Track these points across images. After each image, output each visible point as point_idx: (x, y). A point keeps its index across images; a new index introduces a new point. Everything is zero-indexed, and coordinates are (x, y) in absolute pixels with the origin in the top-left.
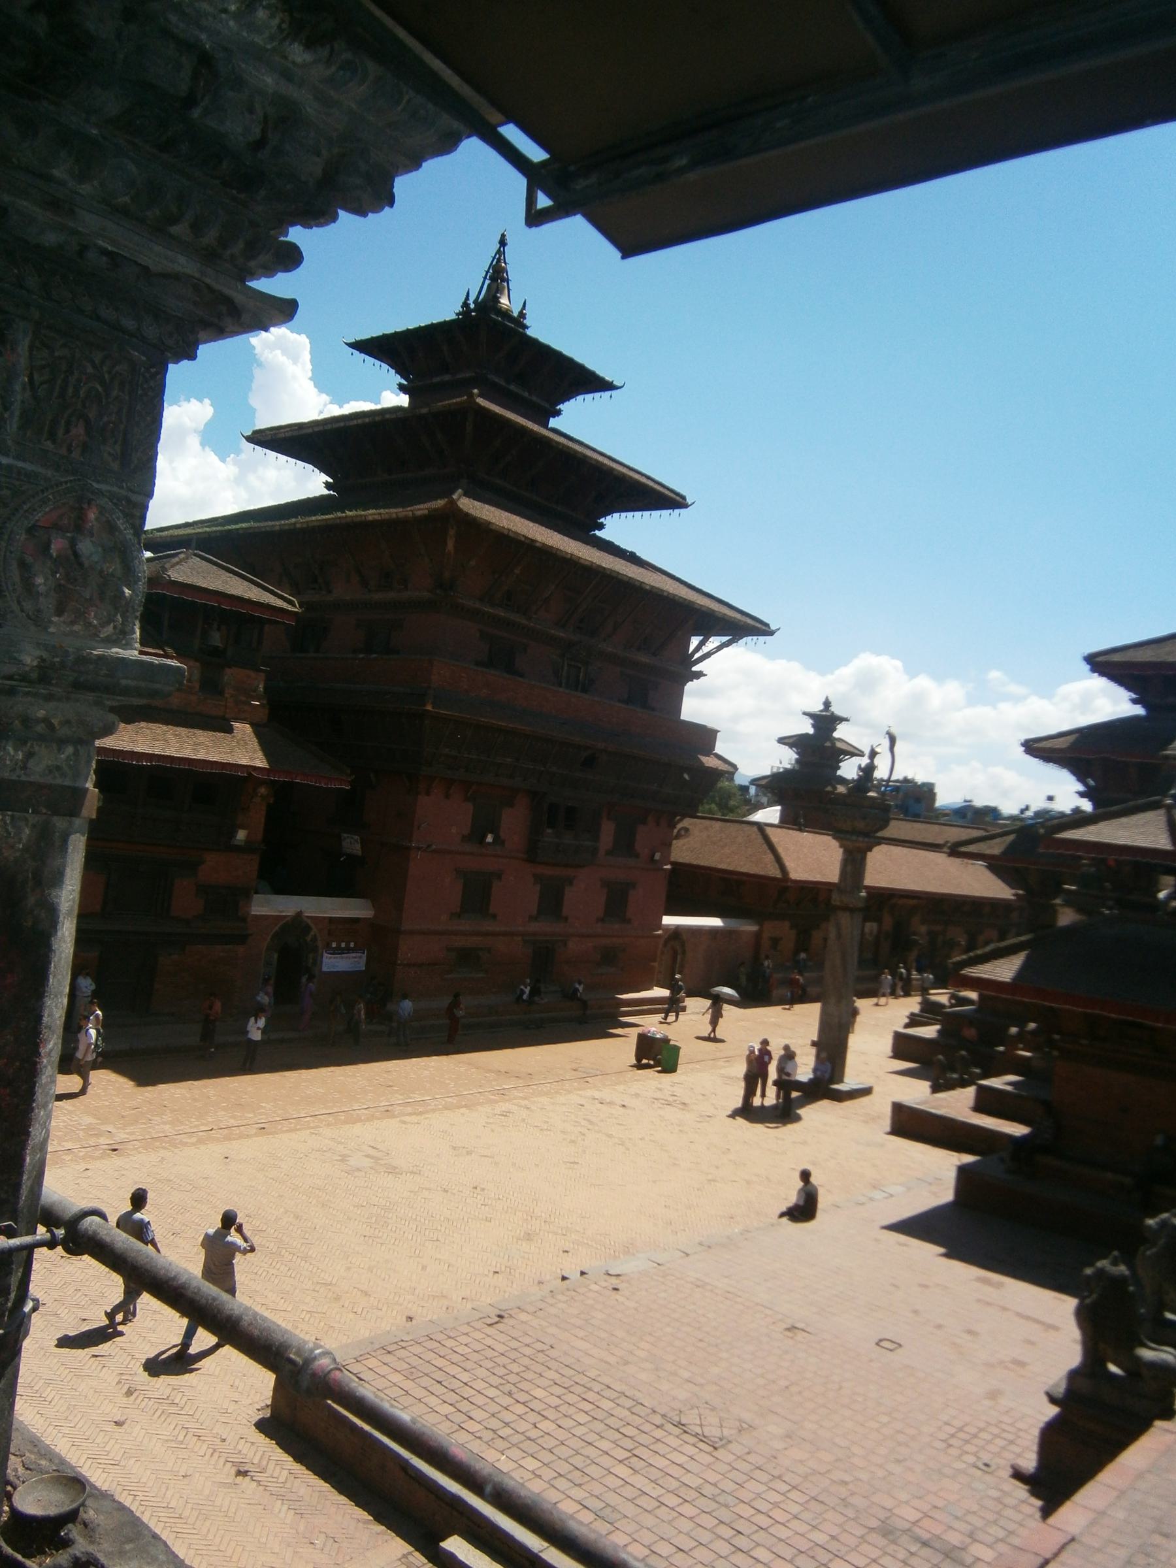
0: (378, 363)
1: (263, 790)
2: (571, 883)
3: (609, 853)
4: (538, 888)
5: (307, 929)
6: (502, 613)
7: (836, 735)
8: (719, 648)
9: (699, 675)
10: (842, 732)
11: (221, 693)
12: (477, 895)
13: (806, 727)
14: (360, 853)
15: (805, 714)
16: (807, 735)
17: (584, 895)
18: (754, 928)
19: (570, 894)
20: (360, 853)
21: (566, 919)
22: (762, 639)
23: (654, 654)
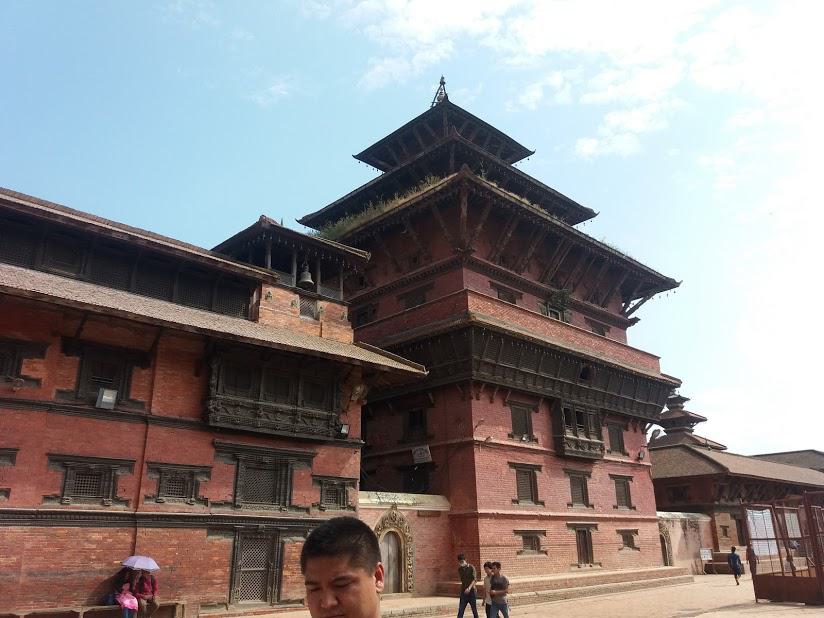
2: (590, 476)
8: (642, 302)
9: (636, 320)
10: (687, 407)
11: (317, 319)
14: (430, 459)
17: (600, 482)
19: (591, 484)
21: (592, 506)
22: (673, 290)
23: (603, 306)
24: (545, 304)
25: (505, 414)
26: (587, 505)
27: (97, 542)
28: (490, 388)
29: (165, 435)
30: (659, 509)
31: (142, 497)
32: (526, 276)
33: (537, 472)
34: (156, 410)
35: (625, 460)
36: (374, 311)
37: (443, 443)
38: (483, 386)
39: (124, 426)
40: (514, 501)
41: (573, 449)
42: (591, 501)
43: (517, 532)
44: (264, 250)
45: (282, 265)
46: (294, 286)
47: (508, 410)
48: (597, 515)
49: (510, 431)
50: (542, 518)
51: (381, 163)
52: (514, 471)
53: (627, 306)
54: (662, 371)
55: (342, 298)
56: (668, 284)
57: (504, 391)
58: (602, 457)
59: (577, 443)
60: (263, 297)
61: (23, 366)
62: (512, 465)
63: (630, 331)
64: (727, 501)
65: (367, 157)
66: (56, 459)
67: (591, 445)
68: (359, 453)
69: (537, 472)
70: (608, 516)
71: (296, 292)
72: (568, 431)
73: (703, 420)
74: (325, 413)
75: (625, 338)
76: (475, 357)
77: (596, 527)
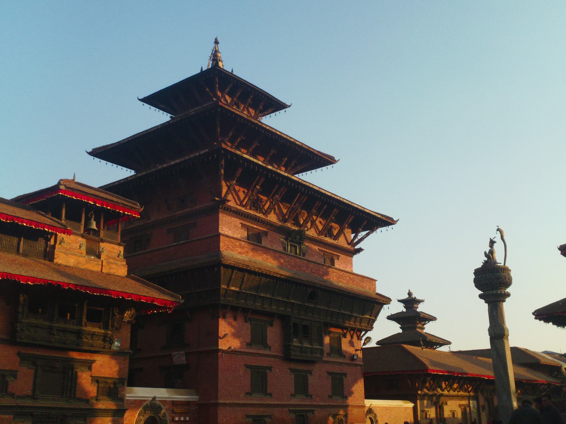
1: (127, 315)
3: (329, 354)
4: (293, 376)
5: (160, 408)
6: (252, 212)
7: (418, 310)
8: (367, 235)
9: (360, 250)
10: (421, 308)
11: (99, 257)
12: (259, 380)
13: (400, 308)
14: (185, 362)
15: (399, 301)
16: (403, 312)
18: (411, 405)
19: (311, 380)
21: (311, 396)
24: (286, 239)
25: (247, 328)
30: (368, 397)
33: (268, 371)
38: (229, 308)
40: (247, 393)
41: (298, 353)
42: (310, 391)
43: (248, 416)
44: (61, 204)
45: (73, 217)
46: (82, 232)
47: (248, 325)
48: (315, 403)
49: (248, 340)
52: (249, 370)
53: (355, 237)
54: (378, 291)
55: (119, 241)
57: (245, 311)
59: (301, 349)
60: (58, 242)
62: (247, 366)
63: (356, 258)
67: (312, 351)
68: (128, 360)
69: (268, 371)
70: (323, 404)
71: (83, 236)
74: (103, 331)
75: (351, 264)
77: (313, 411)
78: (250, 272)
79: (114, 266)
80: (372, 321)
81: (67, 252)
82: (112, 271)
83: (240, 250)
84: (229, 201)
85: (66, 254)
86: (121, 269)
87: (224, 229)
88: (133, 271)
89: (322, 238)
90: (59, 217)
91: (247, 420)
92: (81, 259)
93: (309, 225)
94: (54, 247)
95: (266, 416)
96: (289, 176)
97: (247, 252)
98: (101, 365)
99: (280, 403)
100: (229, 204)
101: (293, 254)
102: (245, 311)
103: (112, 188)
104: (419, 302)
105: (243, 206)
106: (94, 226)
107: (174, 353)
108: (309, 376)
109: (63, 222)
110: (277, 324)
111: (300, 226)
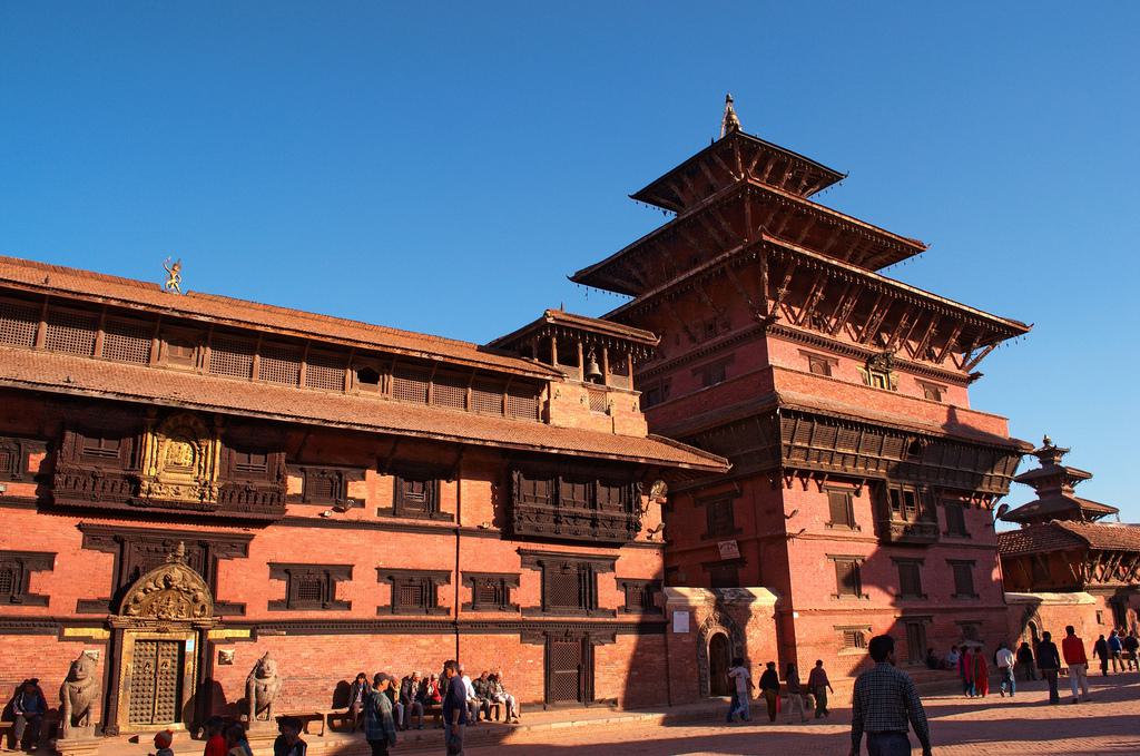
0: (657, 208)
8: (987, 352)
9: (976, 376)
11: (608, 413)
14: (738, 555)
20: (738, 555)
21: (926, 596)
22: (1021, 336)
24: (867, 368)
26: (921, 596)
27: (427, 648)
28: (803, 474)
29: (474, 545)
31: (460, 604)
32: (843, 337)
34: (465, 522)
35: (964, 542)
36: (667, 387)
37: (752, 537)
39: (439, 538)
42: (924, 591)
43: (839, 628)
44: (549, 342)
47: (824, 497)
49: (828, 518)
50: (866, 611)
51: (663, 201)
56: (1012, 330)
57: (818, 476)
58: (936, 540)
61: (349, 489)
64: (1100, 581)
65: (645, 196)
66: (386, 574)
70: (944, 606)
71: (583, 386)
72: (895, 514)
73: (1087, 476)
76: (785, 442)
77: (930, 618)
78: (822, 419)
79: (629, 424)
80: (1006, 481)
81: (564, 408)
82: (628, 432)
83: (802, 387)
84: (778, 318)
85: (563, 411)
86: (637, 426)
87: (776, 360)
88: (652, 429)
89: (918, 361)
90: (550, 361)
91: (838, 632)
92: (584, 417)
93: (897, 343)
94: (547, 404)
95: (863, 627)
96: (864, 272)
97: (814, 390)
98: (627, 563)
99: (881, 607)
100: (779, 322)
101: (879, 387)
102: (818, 476)
103: (617, 316)
104: (1063, 452)
105: (800, 325)
106: (596, 370)
107: (721, 543)
108: (920, 567)
109: (556, 365)
110: (865, 489)
111: (885, 347)
